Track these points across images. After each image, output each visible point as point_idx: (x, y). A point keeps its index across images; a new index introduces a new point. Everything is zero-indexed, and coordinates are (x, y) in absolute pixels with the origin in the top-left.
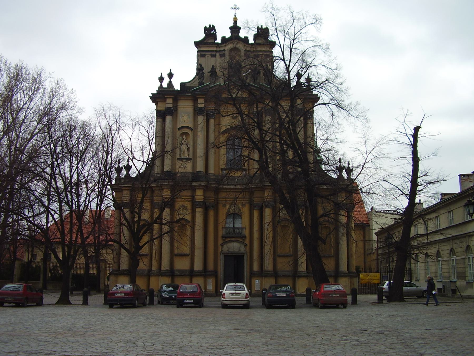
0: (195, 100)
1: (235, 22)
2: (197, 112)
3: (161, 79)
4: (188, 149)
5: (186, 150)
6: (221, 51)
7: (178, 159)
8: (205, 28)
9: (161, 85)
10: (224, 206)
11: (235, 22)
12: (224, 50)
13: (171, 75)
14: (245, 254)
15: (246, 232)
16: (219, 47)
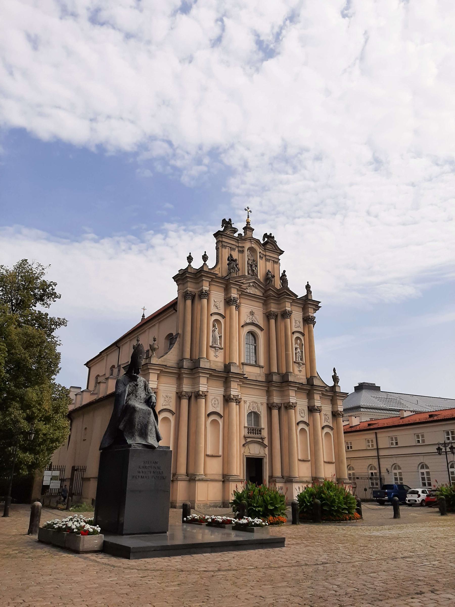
0: (227, 290)
1: (248, 223)
2: (229, 302)
3: (190, 259)
4: (220, 337)
5: (218, 338)
6: (240, 247)
7: (211, 347)
8: (224, 221)
9: (190, 265)
10: (245, 402)
11: (248, 223)
12: (244, 247)
13: (205, 258)
14: (265, 456)
15: (265, 433)
16: (238, 243)
